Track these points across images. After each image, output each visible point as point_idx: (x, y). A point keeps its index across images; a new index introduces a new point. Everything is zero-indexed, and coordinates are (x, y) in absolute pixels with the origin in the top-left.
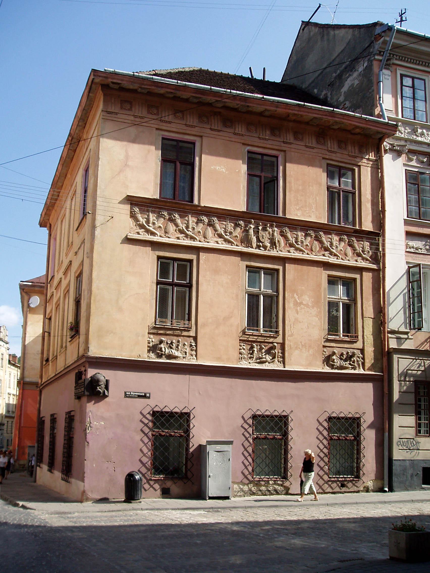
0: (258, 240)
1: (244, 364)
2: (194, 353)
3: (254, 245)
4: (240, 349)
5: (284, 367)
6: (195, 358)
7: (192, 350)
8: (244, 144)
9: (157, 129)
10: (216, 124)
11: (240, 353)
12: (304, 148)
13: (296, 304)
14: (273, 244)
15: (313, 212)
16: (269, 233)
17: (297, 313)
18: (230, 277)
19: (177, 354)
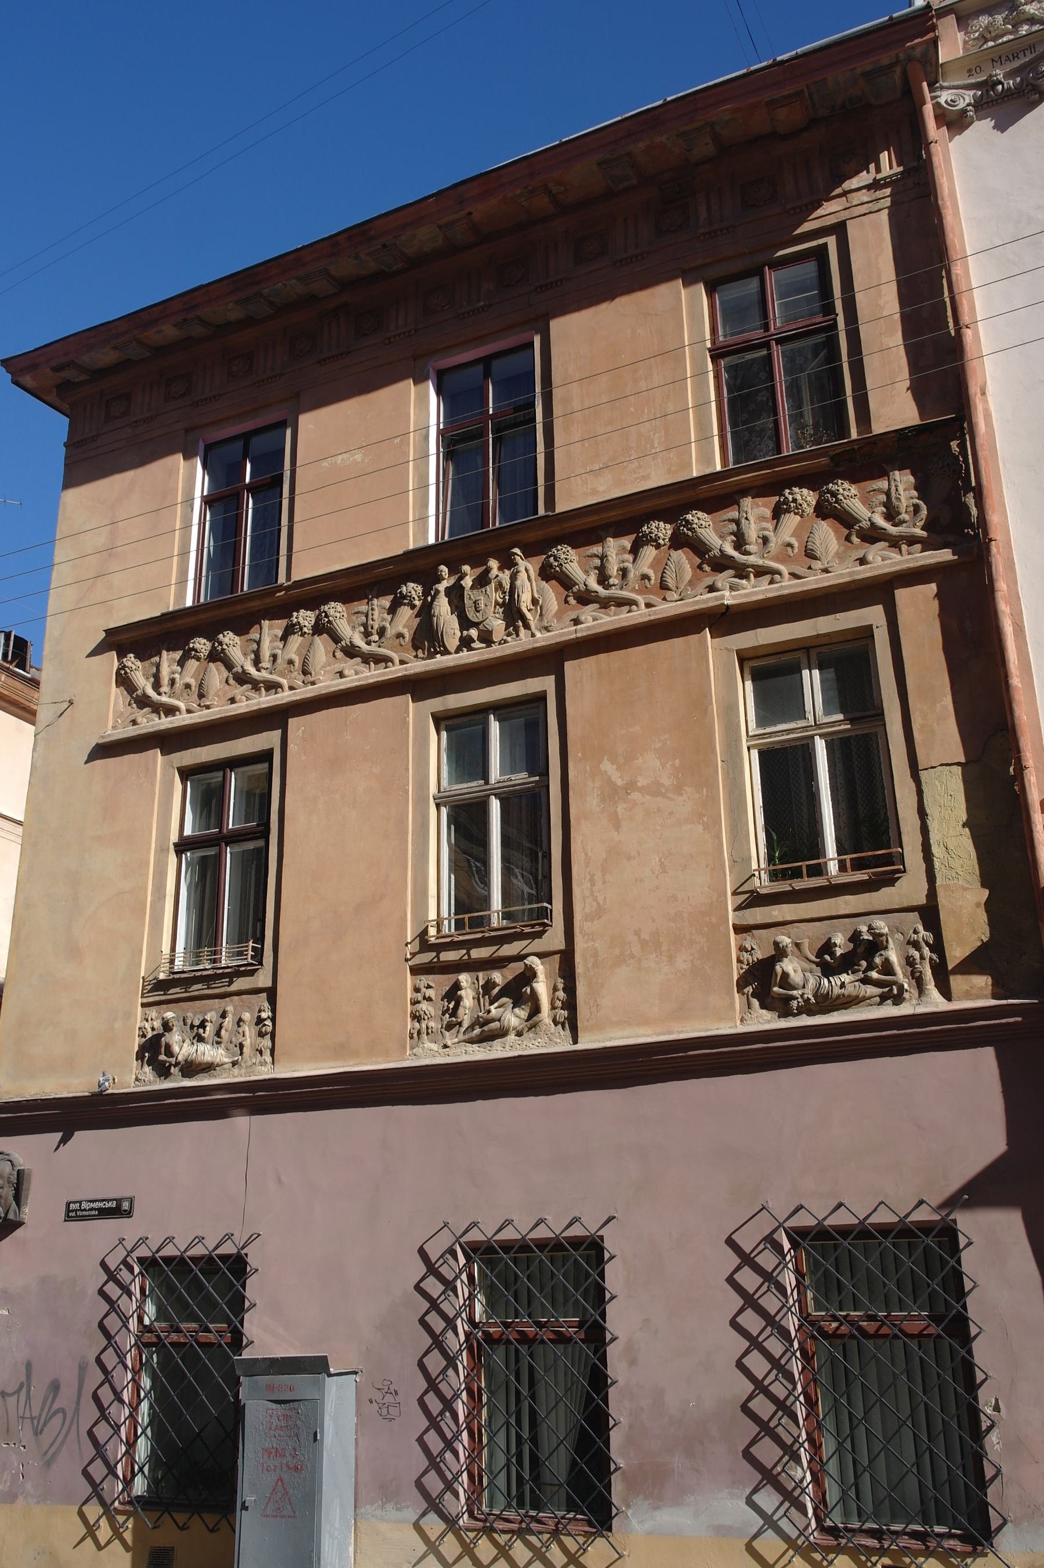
0: (465, 623)
1: (431, 1053)
2: (267, 1042)
3: (452, 643)
4: (415, 1002)
5: (575, 1042)
6: (269, 1059)
7: (261, 1035)
11: (416, 1017)
13: (612, 794)
14: (513, 615)
16: (500, 586)
17: (617, 827)
19: (207, 1052)
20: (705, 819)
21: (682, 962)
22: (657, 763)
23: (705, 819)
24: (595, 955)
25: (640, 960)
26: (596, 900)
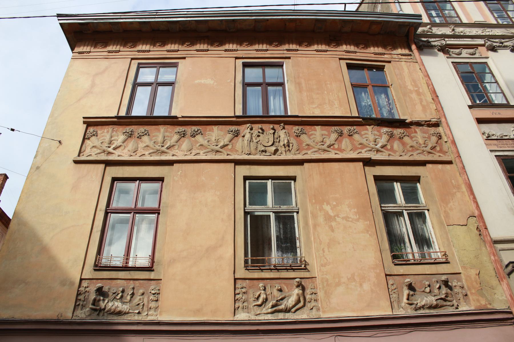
12: (315, 52)
13: (329, 218)
15: (336, 108)
17: (333, 231)
18: (218, 193)
20: (370, 232)
21: (366, 286)
22: (348, 210)
23: (370, 232)
24: (327, 280)
25: (347, 285)
26: (326, 258)
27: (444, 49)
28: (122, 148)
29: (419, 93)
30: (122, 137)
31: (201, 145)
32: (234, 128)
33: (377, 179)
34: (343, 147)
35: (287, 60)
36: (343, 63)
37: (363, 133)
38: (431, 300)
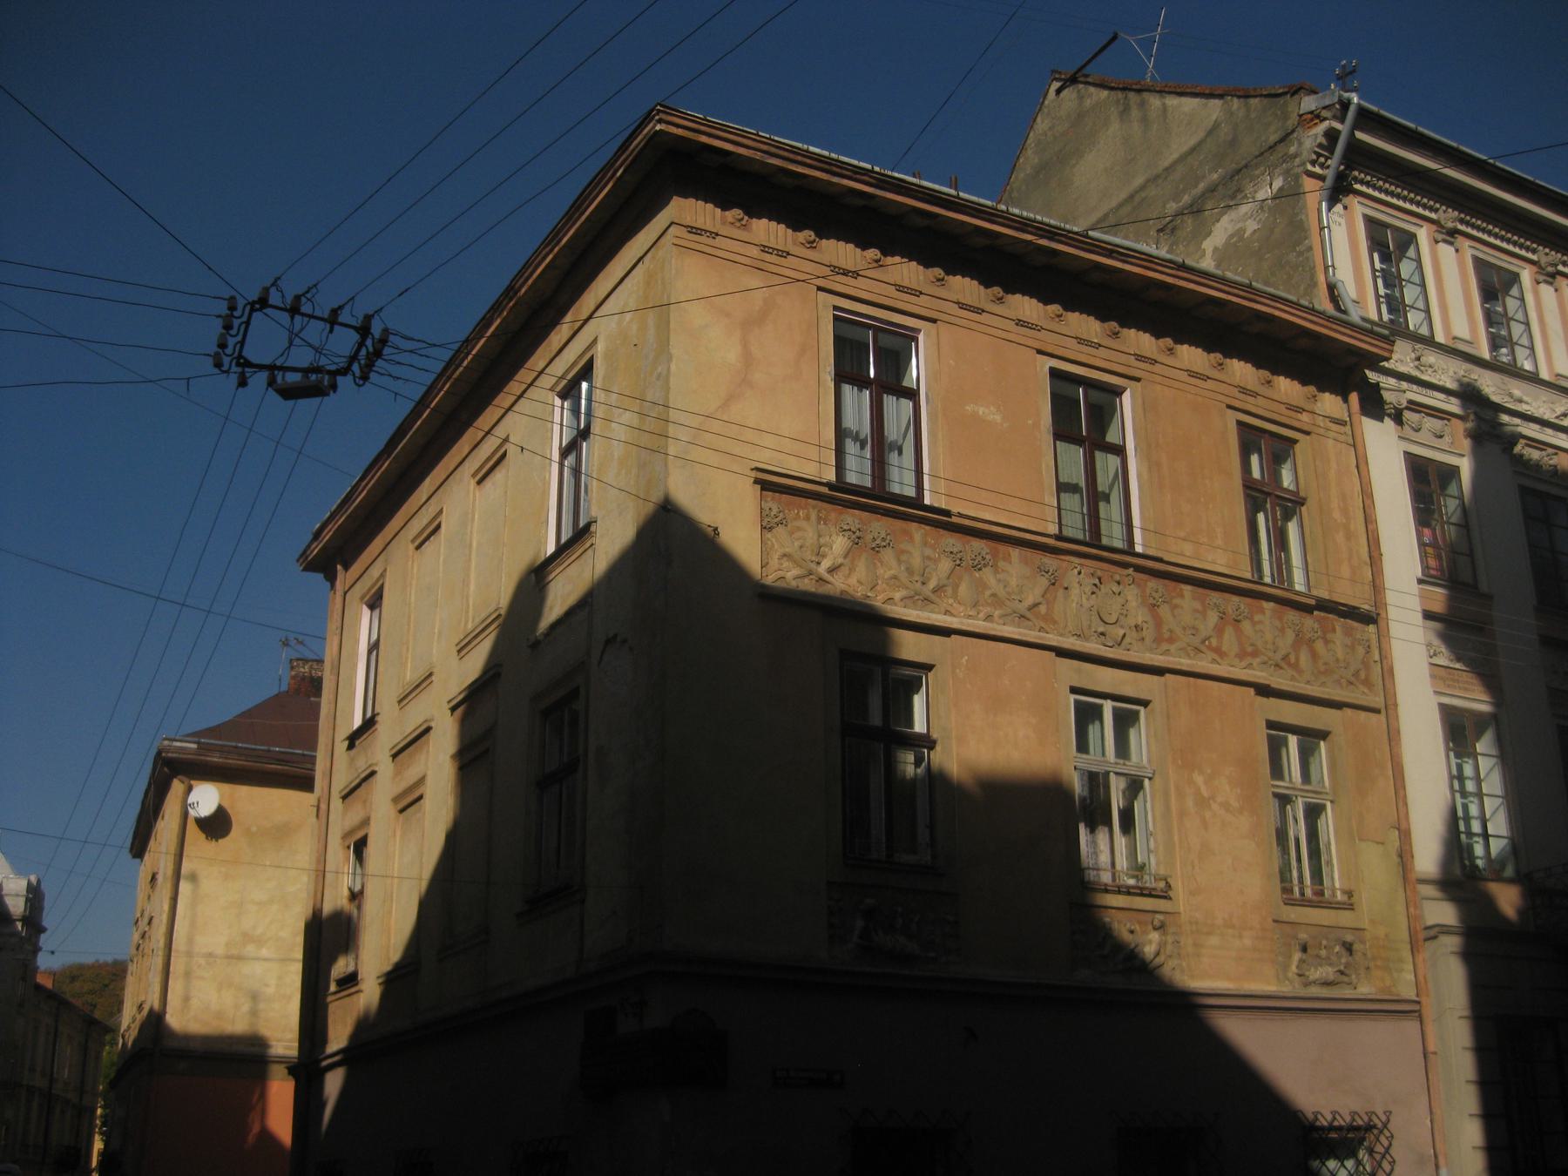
8: (1039, 352)
9: (820, 289)
10: (964, 287)
12: (1184, 376)
13: (1202, 803)
17: (1206, 828)
27: (1398, 418)
28: (845, 570)
29: (1349, 536)
30: (839, 544)
31: (994, 595)
32: (1050, 561)
33: (1271, 725)
34: (1224, 649)
35: (1133, 383)
36: (1232, 417)
37: (1257, 618)
38: (1327, 972)
